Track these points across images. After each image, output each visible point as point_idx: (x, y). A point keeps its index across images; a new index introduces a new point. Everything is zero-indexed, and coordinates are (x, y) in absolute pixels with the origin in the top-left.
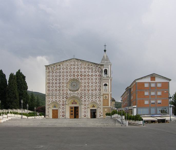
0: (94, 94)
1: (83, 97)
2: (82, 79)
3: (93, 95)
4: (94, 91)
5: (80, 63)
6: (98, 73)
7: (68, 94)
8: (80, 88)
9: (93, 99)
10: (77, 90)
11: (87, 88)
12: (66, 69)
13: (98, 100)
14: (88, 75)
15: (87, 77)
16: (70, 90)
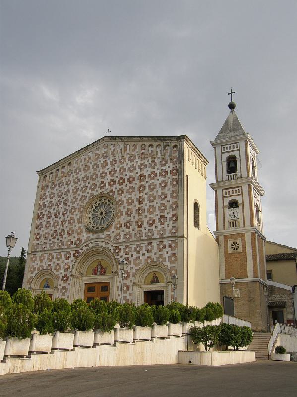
0: (156, 236)
1: (122, 247)
2: (123, 192)
3: (151, 239)
4: (157, 224)
5: (122, 145)
6: (171, 165)
7: (83, 241)
8: (116, 220)
9: (152, 254)
10: (107, 228)
11: (135, 217)
12: (84, 170)
13: (167, 256)
14: (141, 175)
15: (136, 184)
16: (89, 230)
